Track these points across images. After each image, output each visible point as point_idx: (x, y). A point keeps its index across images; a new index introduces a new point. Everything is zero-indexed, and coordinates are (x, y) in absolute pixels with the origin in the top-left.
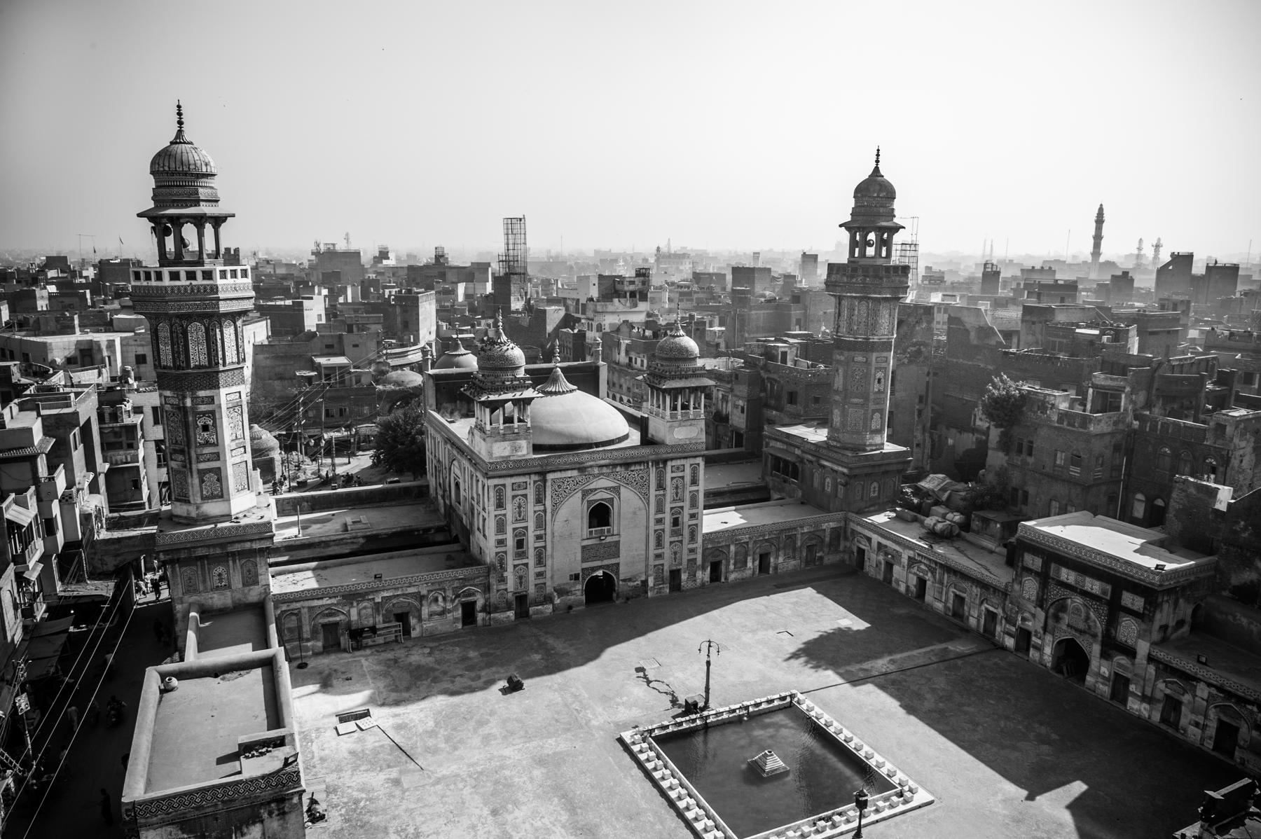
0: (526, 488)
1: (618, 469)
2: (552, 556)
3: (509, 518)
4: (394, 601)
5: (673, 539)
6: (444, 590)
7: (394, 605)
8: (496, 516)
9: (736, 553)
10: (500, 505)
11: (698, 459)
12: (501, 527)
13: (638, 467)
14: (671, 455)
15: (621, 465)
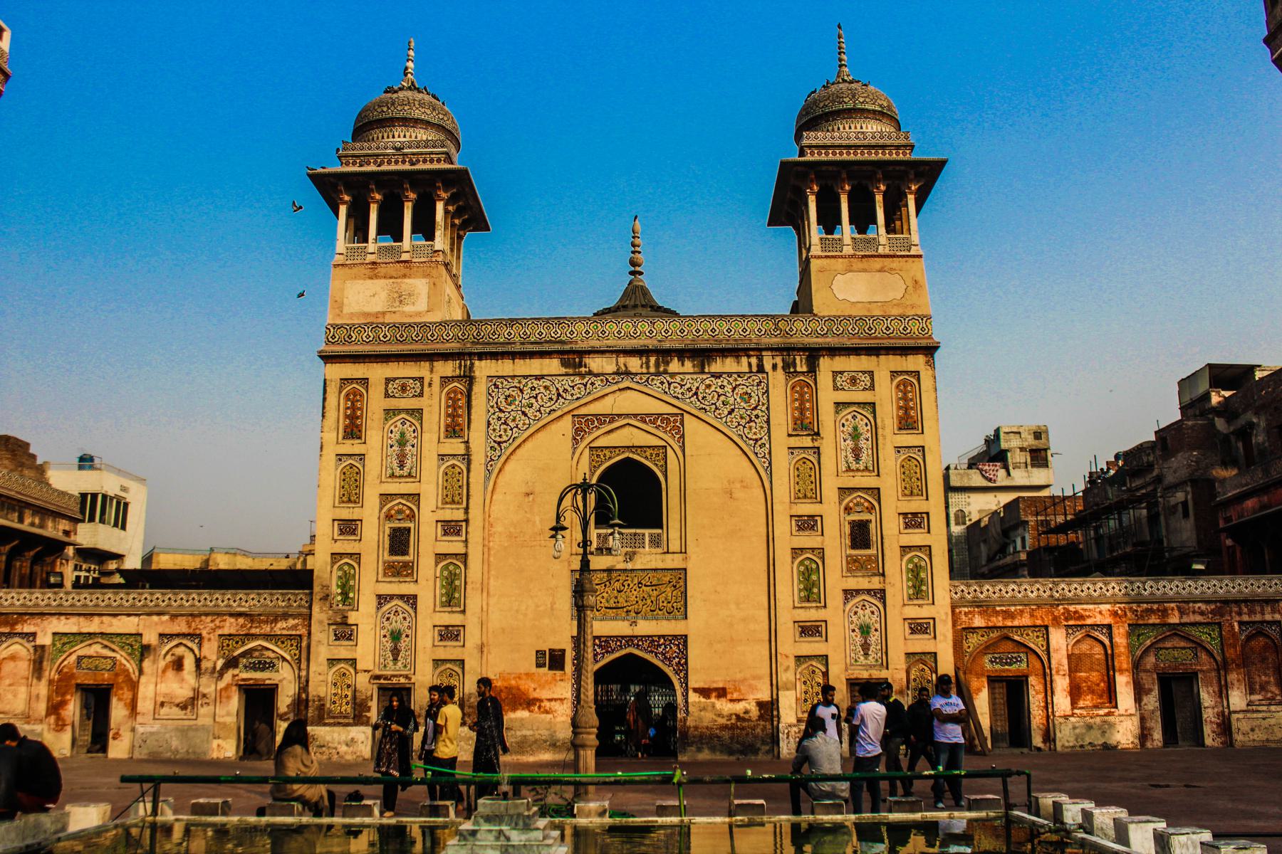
0: (421, 395)
1: (674, 366)
2: (485, 588)
3: (373, 467)
4: (83, 650)
5: (852, 583)
6: (197, 637)
7: (80, 658)
8: (340, 457)
9: (1075, 662)
10: (353, 430)
11: (910, 358)
12: (351, 492)
13: (729, 365)
14: (830, 341)
15: (682, 354)
